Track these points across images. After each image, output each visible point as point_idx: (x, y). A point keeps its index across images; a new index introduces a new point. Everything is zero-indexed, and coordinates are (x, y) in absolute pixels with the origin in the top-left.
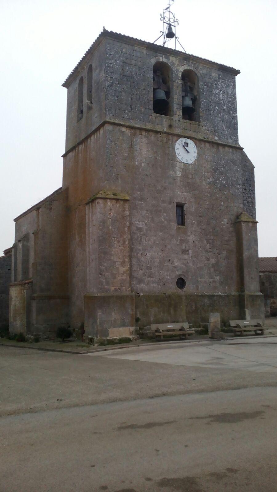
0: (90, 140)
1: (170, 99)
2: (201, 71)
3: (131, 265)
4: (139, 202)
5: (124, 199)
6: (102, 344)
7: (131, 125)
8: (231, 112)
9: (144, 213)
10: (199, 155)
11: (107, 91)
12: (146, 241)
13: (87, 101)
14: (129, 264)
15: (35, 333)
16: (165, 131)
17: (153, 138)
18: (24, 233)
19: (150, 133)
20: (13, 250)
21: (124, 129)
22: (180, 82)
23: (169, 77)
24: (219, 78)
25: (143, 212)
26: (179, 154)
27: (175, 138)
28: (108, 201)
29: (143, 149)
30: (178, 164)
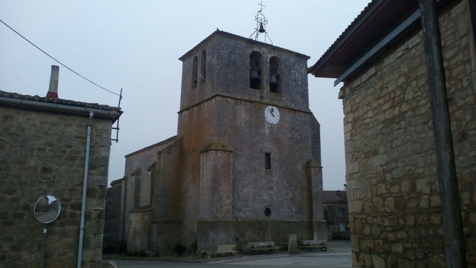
0: (204, 104)
1: (261, 77)
2: (283, 57)
3: (234, 198)
4: (239, 152)
5: (229, 150)
6: (213, 256)
7: (235, 97)
8: (304, 86)
9: (243, 160)
10: (282, 118)
11: (218, 72)
12: (244, 181)
13: (201, 76)
14: (232, 198)
15: (155, 250)
16: (258, 101)
17: (249, 106)
18: (135, 168)
19: (248, 102)
20: (124, 182)
21: (229, 100)
22: (268, 65)
23: (260, 61)
24: (296, 62)
25: (242, 159)
26: (268, 117)
27: (265, 106)
28: (219, 151)
29: (243, 114)
30: (267, 124)
